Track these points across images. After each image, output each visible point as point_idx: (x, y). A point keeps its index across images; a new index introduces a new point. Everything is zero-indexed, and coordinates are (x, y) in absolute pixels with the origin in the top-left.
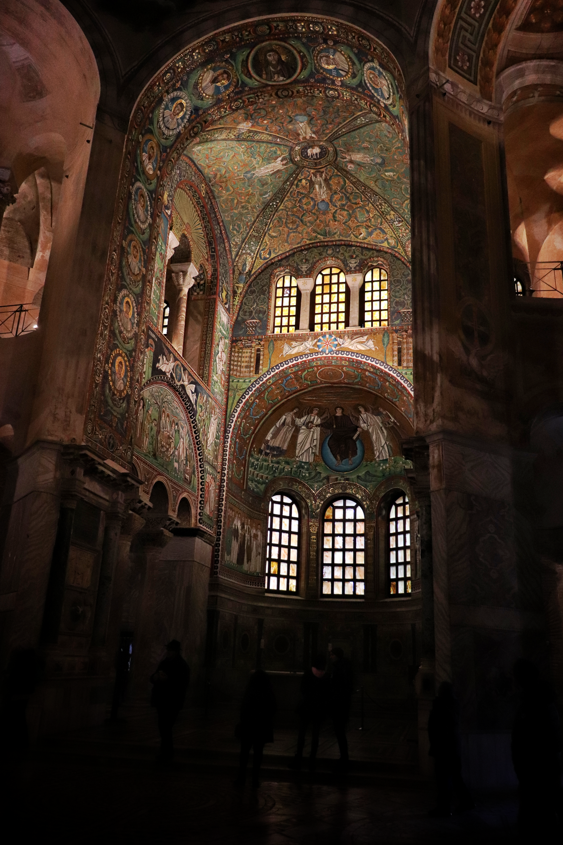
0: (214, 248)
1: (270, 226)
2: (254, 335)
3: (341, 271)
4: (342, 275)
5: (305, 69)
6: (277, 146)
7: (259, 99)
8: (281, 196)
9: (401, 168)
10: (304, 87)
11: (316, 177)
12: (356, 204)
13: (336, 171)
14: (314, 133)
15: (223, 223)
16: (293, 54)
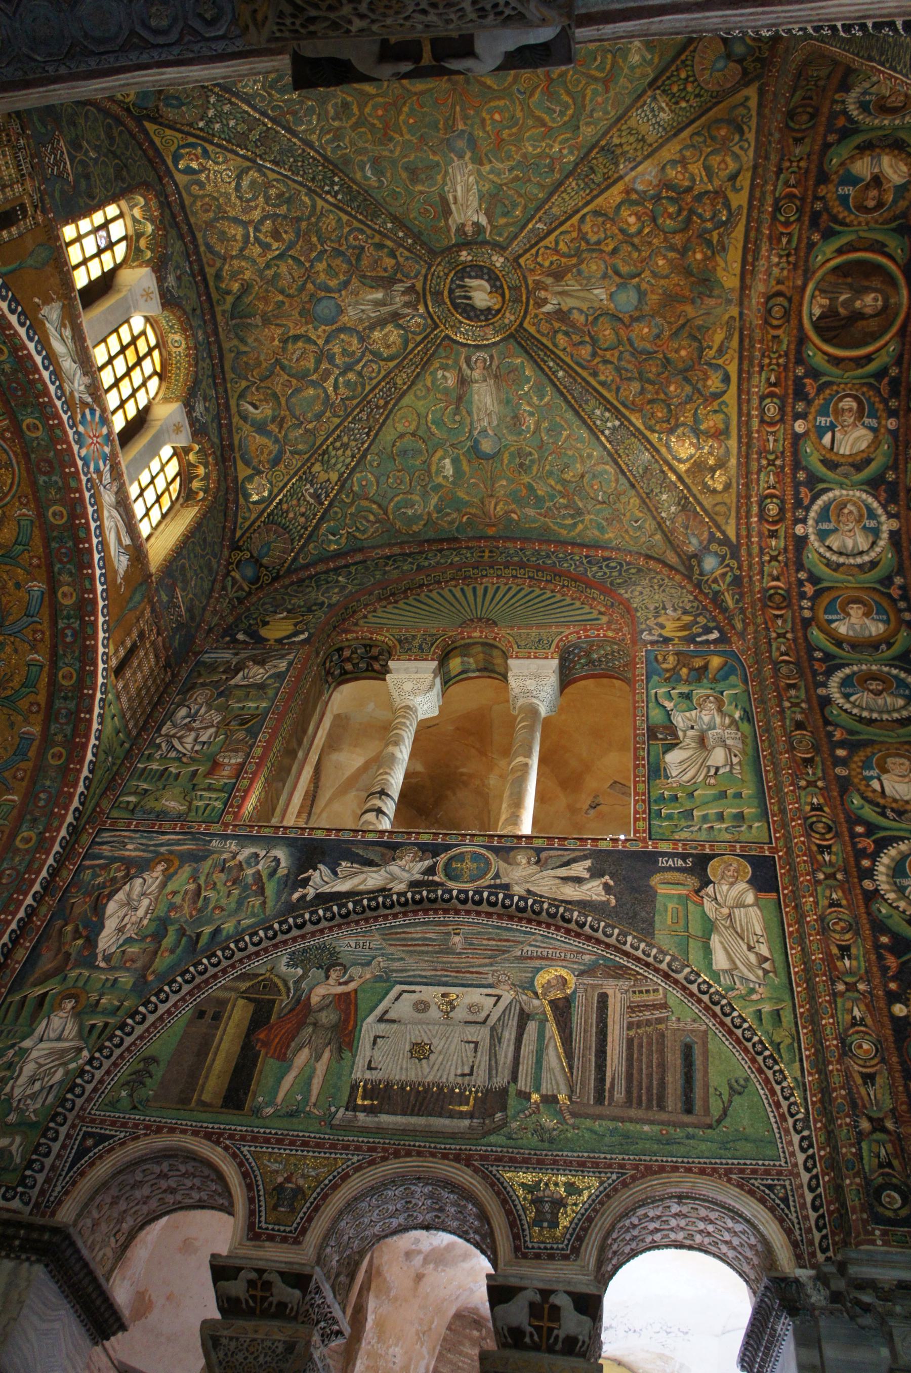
1: (268, 172)
2: (45, 180)
3: (161, 376)
4: (155, 380)
7: (780, 257)
8: (355, 204)
9: (468, 493)
10: (786, 354)
11: (404, 293)
13: (419, 338)
14: (559, 311)
16: (865, 344)
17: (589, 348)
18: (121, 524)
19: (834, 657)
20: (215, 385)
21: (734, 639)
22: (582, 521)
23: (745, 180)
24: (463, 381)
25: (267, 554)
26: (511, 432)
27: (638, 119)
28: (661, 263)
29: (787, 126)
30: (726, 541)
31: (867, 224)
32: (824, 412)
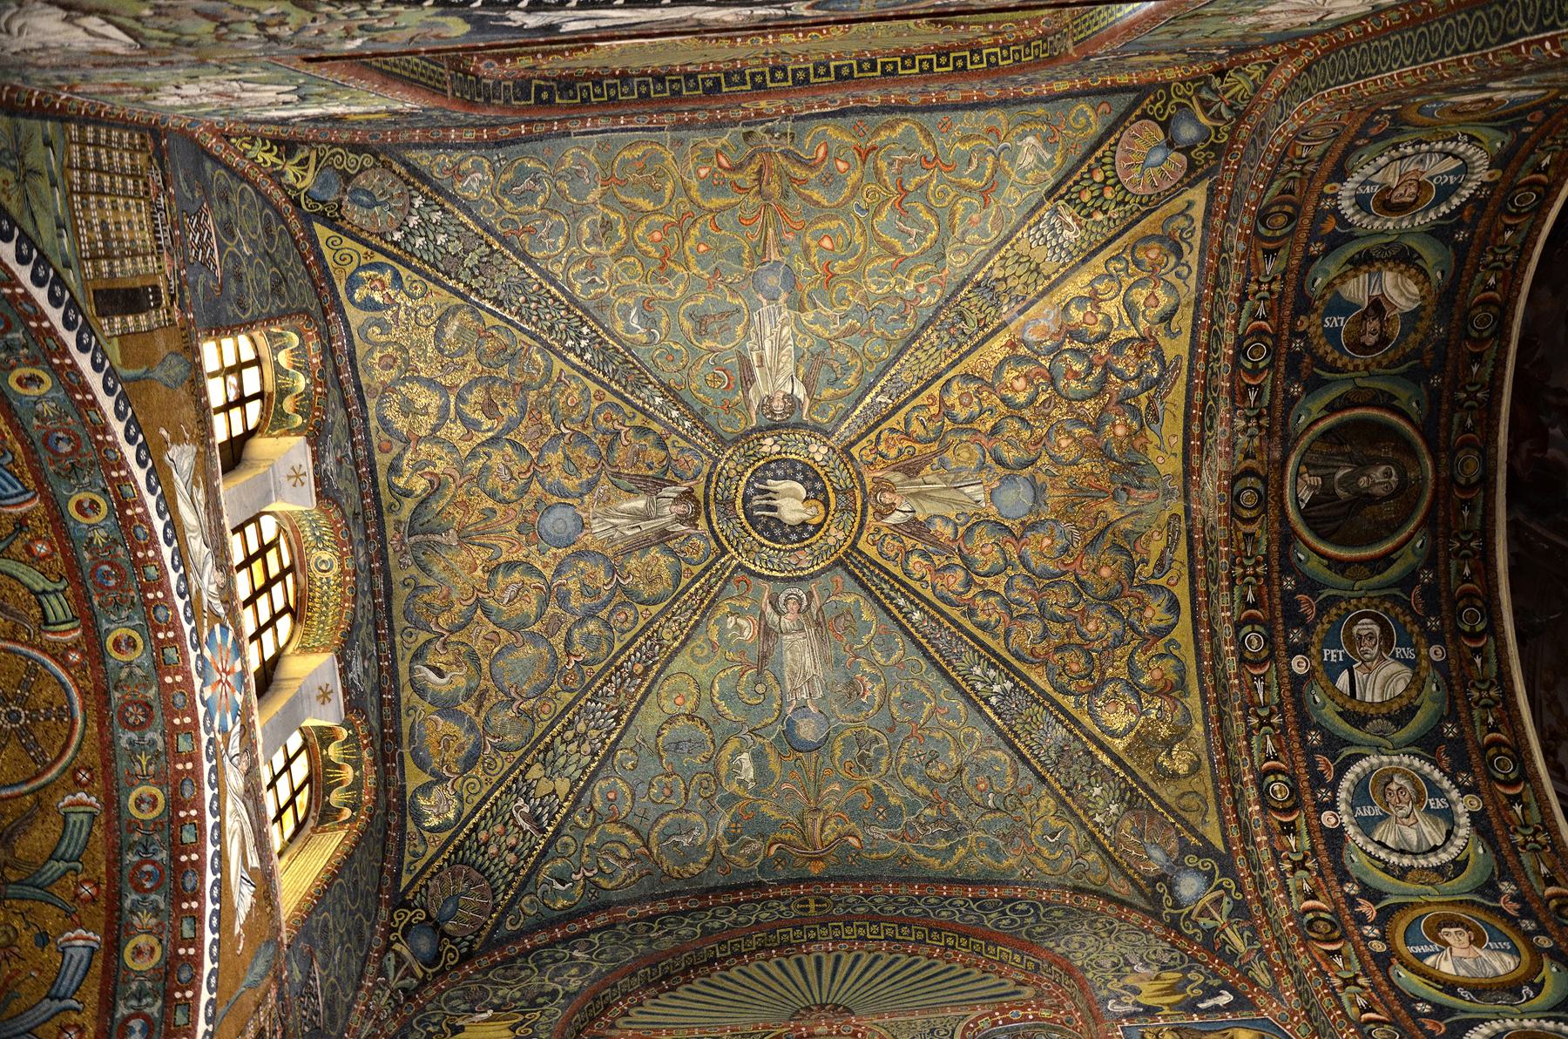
0: (551, 101)
5: (1329, 567)
6: (857, 394)
7: (1248, 419)
10: (1267, 559)
12: (568, 642)
13: (697, 570)
15: (559, 135)
16: (1380, 539)
17: (961, 574)
18: (248, 828)
19: (1452, 1011)
20: (377, 636)
21: (1261, 1000)
22: (964, 843)
23: (1184, 320)
24: (767, 632)
25: (452, 915)
26: (844, 708)
27: (1025, 241)
28: (1064, 443)
29: (1256, 232)
30: (1207, 850)
31: (1367, 368)
32: (1331, 641)
